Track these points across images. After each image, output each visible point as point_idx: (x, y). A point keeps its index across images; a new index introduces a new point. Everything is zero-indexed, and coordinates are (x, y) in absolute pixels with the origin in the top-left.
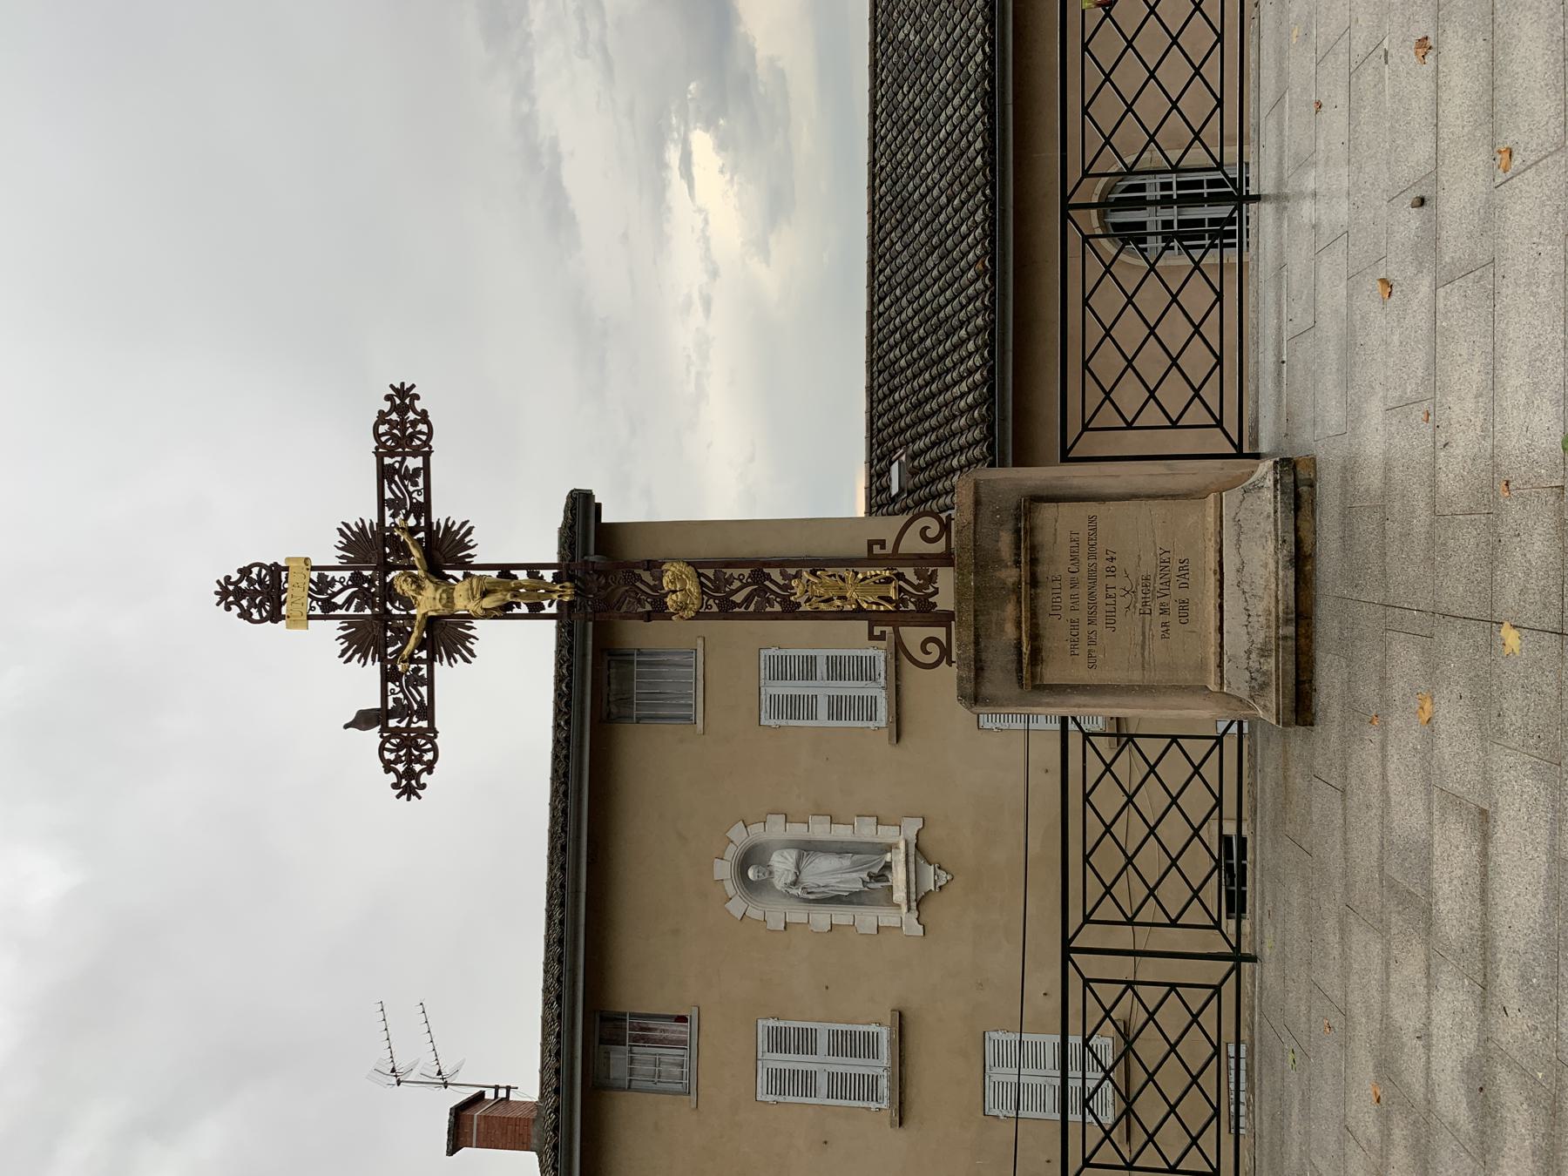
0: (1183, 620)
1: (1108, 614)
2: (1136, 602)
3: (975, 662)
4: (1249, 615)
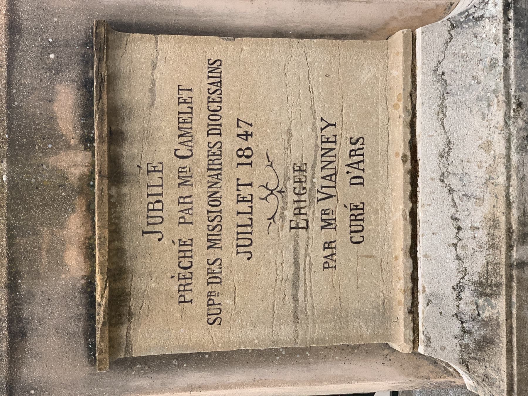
0: (357, 237)
1: (240, 230)
2: (284, 209)
3: (10, 322)
4: (459, 229)
